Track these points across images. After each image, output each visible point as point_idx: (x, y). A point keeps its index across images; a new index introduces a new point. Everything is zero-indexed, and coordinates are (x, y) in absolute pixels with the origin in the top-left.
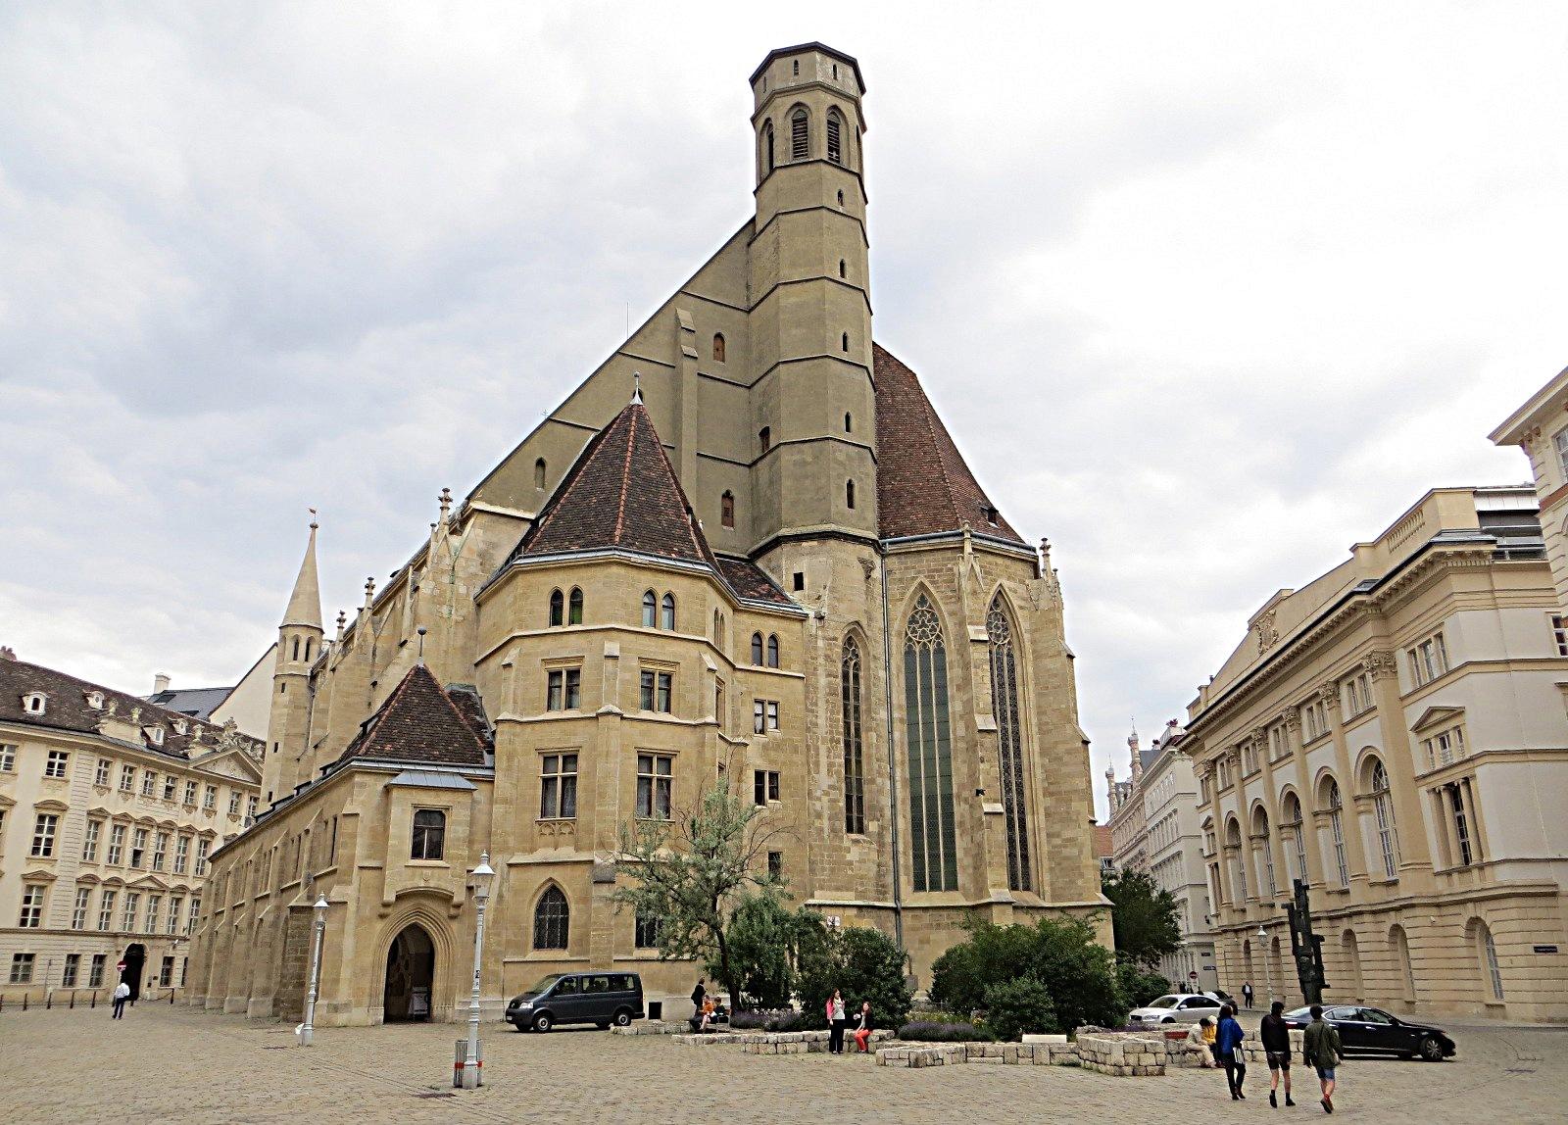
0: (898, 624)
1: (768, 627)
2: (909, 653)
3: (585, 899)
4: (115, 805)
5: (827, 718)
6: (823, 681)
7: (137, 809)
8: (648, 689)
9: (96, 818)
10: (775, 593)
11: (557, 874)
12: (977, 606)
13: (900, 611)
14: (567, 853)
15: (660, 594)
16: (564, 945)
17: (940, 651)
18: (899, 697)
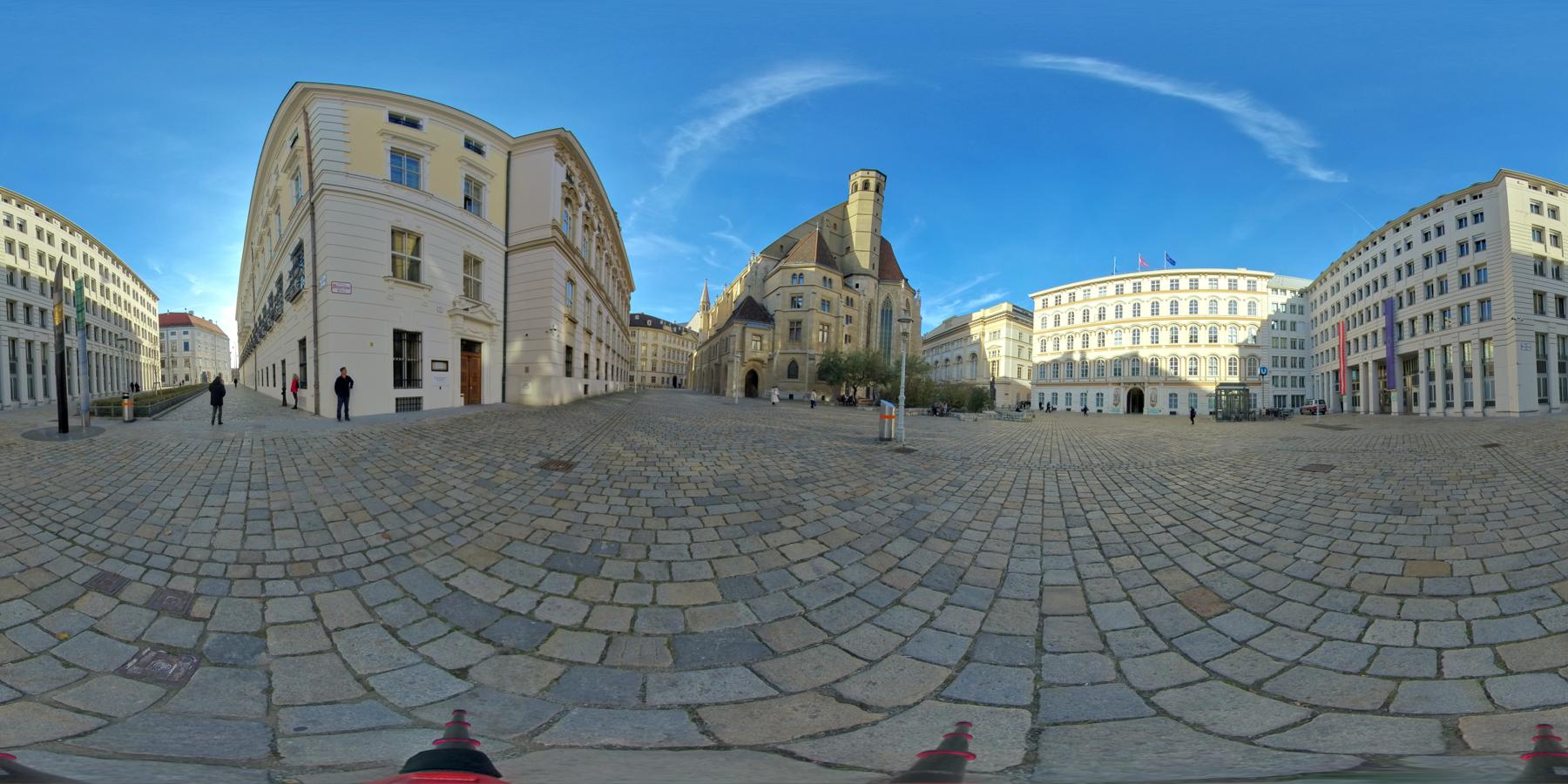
0: (881, 302)
1: (851, 295)
2: (883, 311)
3: (804, 364)
4: (667, 345)
5: (863, 323)
6: (863, 313)
7: (672, 345)
8: (823, 304)
9: (664, 348)
10: (851, 288)
11: (794, 356)
12: (903, 300)
13: (882, 299)
14: (798, 350)
15: (828, 277)
16: (797, 377)
17: (891, 311)
18: (879, 321)
